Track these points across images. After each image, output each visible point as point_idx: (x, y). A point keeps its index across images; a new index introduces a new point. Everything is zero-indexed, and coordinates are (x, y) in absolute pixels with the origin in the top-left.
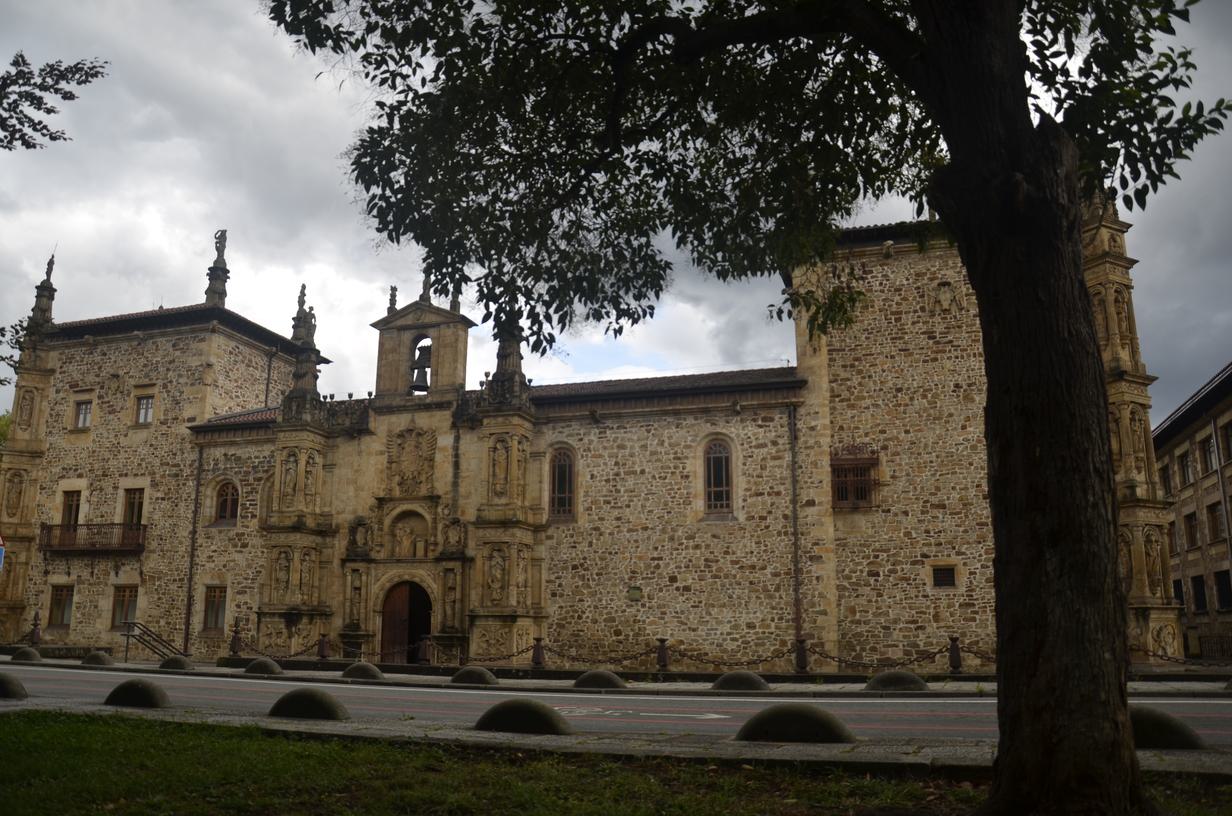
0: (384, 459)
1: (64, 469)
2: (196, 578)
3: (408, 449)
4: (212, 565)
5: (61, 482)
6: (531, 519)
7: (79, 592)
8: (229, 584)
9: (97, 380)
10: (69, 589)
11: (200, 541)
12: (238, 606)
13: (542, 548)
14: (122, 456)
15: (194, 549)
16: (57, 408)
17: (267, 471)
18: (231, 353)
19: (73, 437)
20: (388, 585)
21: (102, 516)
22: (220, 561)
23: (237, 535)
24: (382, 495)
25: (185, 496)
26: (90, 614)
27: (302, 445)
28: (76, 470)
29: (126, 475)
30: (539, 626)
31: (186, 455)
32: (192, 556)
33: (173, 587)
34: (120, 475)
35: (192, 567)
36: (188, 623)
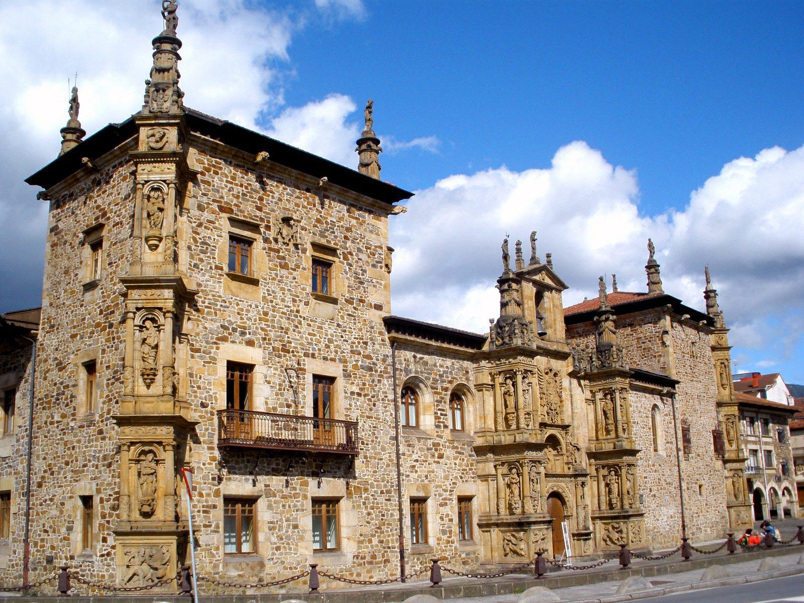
1: (222, 326)
5: (223, 346)
8: (432, 494)
9: (258, 213)
10: (250, 501)
11: (402, 449)
12: (442, 518)
14: (304, 328)
17: (450, 382)
19: (234, 284)
21: (289, 406)
22: (422, 470)
23: (434, 445)
25: (381, 396)
26: (288, 538)
28: (243, 334)
29: (313, 356)
31: (377, 346)
32: (398, 465)
33: (381, 499)
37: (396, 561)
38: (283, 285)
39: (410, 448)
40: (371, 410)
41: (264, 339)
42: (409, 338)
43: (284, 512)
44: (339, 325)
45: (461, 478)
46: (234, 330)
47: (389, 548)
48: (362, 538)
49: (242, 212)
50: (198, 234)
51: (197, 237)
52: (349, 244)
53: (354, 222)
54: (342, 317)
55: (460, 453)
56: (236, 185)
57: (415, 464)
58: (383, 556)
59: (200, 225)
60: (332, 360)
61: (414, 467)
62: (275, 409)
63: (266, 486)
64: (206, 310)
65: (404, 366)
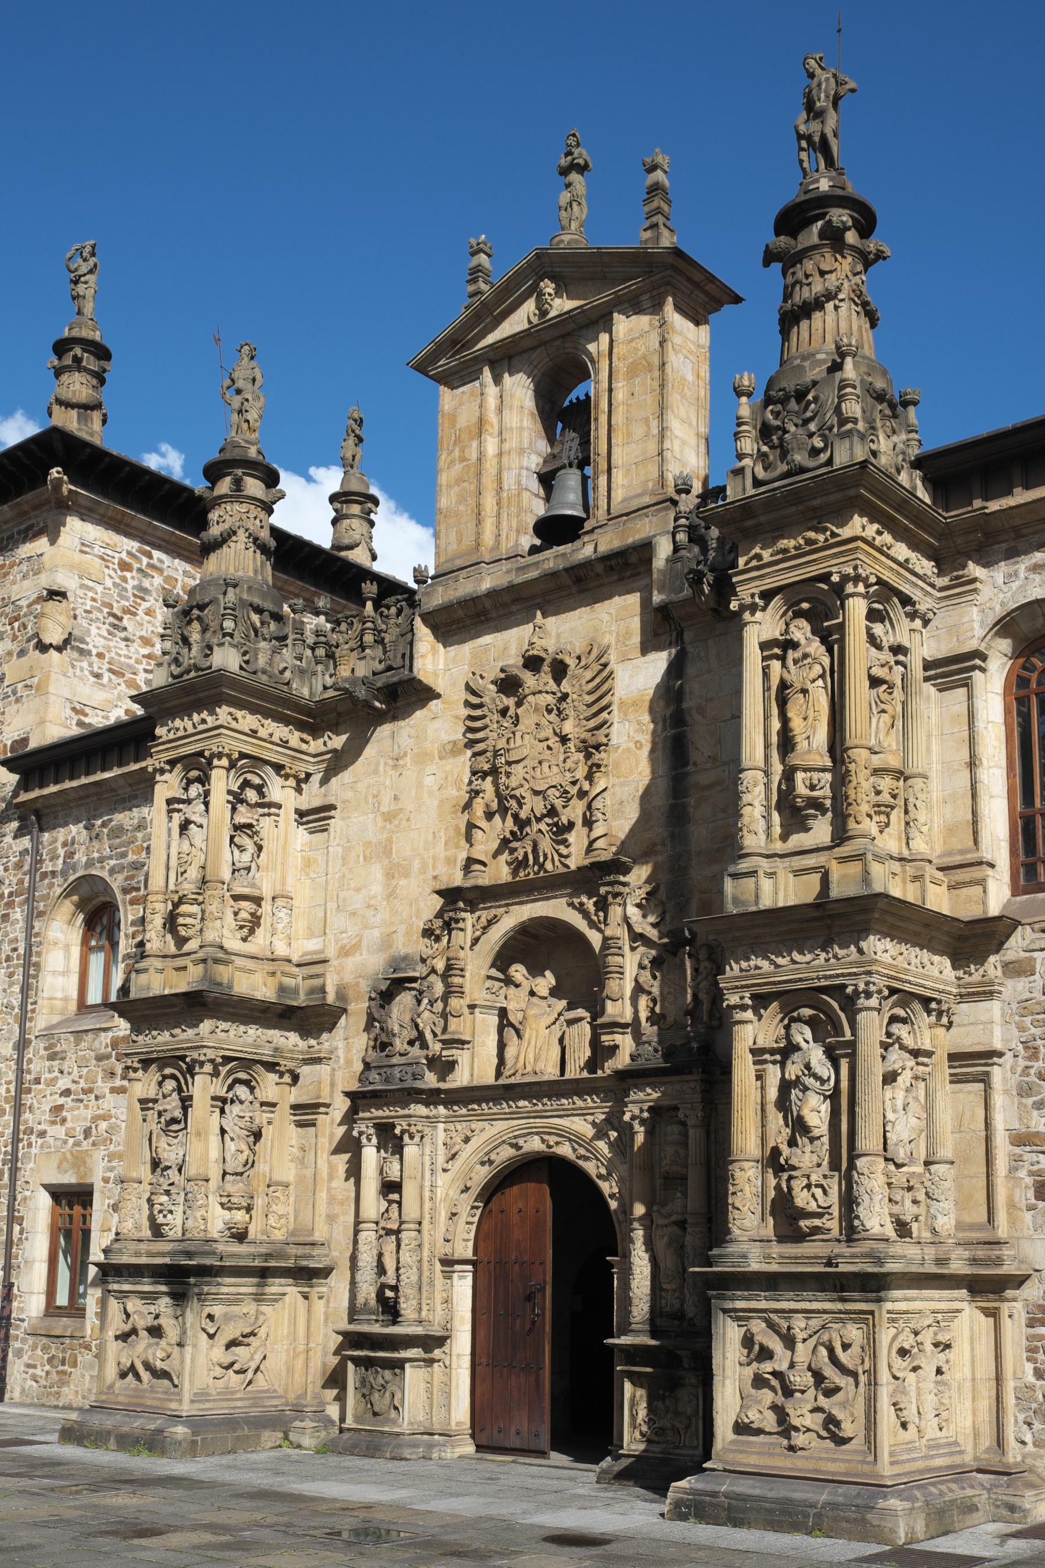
0: (462, 764)
2: (27, 1169)
3: (528, 721)
4: (59, 1131)
6: (939, 900)
13: (994, 1008)
15: (21, 1089)
18: (124, 566)
20: (482, 1174)
22: (78, 1117)
24: (457, 880)
27: (212, 746)
30: (992, 1313)
32: (18, 1108)
35: (16, 1140)
39: (56, 1063)
42: (75, 783)
57: (61, 1101)
61: (59, 1108)
65: (61, 861)
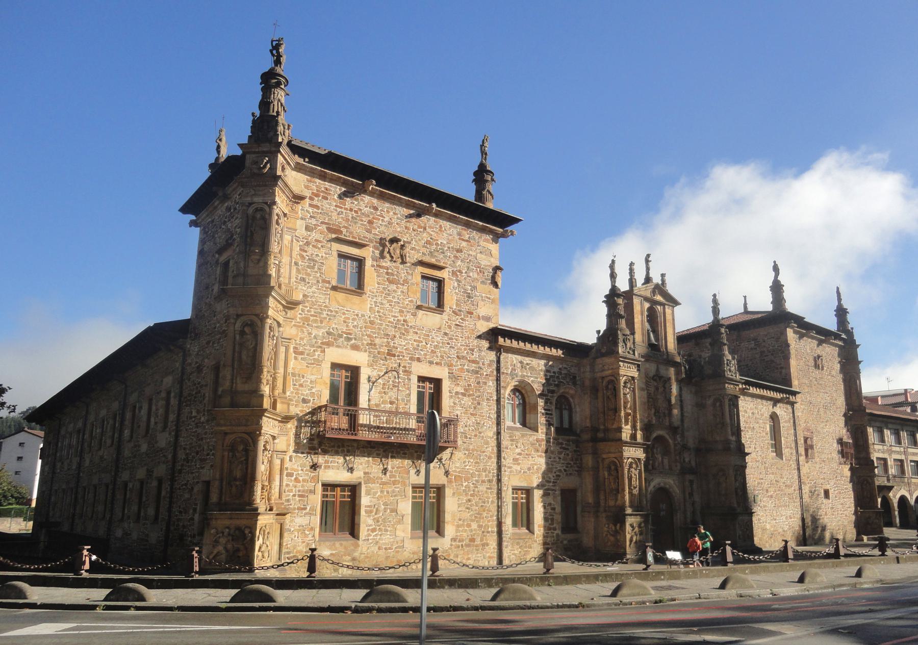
1: (329, 333)
2: (505, 479)
4: (518, 468)
7: (368, 493)
14: (411, 336)
16: (310, 250)
21: (391, 403)
28: (349, 339)
29: (419, 360)
31: (483, 353)
32: (499, 457)
33: (482, 488)
34: (412, 359)
36: (500, 524)
37: (493, 544)
38: (390, 298)
40: (475, 408)
41: (371, 344)
43: (381, 497)
44: (446, 334)
45: (565, 470)
46: (341, 336)
47: (488, 532)
48: (461, 522)
49: (351, 233)
50: (306, 252)
51: (305, 254)
52: (459, 263)
53: (464, 244)
54: (450, 327)
55: (564, 449)
56: (346, 209)
58: (481, 540)
59: (308, 244)
60: (437, 363)
62: (377, 405)
63: (365, 473)
64: (312, 318)
